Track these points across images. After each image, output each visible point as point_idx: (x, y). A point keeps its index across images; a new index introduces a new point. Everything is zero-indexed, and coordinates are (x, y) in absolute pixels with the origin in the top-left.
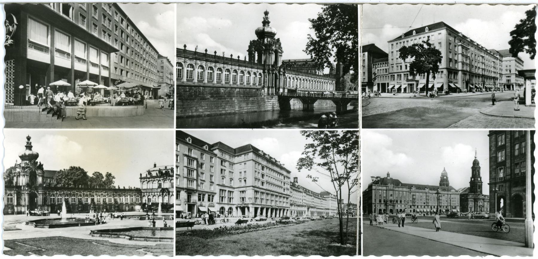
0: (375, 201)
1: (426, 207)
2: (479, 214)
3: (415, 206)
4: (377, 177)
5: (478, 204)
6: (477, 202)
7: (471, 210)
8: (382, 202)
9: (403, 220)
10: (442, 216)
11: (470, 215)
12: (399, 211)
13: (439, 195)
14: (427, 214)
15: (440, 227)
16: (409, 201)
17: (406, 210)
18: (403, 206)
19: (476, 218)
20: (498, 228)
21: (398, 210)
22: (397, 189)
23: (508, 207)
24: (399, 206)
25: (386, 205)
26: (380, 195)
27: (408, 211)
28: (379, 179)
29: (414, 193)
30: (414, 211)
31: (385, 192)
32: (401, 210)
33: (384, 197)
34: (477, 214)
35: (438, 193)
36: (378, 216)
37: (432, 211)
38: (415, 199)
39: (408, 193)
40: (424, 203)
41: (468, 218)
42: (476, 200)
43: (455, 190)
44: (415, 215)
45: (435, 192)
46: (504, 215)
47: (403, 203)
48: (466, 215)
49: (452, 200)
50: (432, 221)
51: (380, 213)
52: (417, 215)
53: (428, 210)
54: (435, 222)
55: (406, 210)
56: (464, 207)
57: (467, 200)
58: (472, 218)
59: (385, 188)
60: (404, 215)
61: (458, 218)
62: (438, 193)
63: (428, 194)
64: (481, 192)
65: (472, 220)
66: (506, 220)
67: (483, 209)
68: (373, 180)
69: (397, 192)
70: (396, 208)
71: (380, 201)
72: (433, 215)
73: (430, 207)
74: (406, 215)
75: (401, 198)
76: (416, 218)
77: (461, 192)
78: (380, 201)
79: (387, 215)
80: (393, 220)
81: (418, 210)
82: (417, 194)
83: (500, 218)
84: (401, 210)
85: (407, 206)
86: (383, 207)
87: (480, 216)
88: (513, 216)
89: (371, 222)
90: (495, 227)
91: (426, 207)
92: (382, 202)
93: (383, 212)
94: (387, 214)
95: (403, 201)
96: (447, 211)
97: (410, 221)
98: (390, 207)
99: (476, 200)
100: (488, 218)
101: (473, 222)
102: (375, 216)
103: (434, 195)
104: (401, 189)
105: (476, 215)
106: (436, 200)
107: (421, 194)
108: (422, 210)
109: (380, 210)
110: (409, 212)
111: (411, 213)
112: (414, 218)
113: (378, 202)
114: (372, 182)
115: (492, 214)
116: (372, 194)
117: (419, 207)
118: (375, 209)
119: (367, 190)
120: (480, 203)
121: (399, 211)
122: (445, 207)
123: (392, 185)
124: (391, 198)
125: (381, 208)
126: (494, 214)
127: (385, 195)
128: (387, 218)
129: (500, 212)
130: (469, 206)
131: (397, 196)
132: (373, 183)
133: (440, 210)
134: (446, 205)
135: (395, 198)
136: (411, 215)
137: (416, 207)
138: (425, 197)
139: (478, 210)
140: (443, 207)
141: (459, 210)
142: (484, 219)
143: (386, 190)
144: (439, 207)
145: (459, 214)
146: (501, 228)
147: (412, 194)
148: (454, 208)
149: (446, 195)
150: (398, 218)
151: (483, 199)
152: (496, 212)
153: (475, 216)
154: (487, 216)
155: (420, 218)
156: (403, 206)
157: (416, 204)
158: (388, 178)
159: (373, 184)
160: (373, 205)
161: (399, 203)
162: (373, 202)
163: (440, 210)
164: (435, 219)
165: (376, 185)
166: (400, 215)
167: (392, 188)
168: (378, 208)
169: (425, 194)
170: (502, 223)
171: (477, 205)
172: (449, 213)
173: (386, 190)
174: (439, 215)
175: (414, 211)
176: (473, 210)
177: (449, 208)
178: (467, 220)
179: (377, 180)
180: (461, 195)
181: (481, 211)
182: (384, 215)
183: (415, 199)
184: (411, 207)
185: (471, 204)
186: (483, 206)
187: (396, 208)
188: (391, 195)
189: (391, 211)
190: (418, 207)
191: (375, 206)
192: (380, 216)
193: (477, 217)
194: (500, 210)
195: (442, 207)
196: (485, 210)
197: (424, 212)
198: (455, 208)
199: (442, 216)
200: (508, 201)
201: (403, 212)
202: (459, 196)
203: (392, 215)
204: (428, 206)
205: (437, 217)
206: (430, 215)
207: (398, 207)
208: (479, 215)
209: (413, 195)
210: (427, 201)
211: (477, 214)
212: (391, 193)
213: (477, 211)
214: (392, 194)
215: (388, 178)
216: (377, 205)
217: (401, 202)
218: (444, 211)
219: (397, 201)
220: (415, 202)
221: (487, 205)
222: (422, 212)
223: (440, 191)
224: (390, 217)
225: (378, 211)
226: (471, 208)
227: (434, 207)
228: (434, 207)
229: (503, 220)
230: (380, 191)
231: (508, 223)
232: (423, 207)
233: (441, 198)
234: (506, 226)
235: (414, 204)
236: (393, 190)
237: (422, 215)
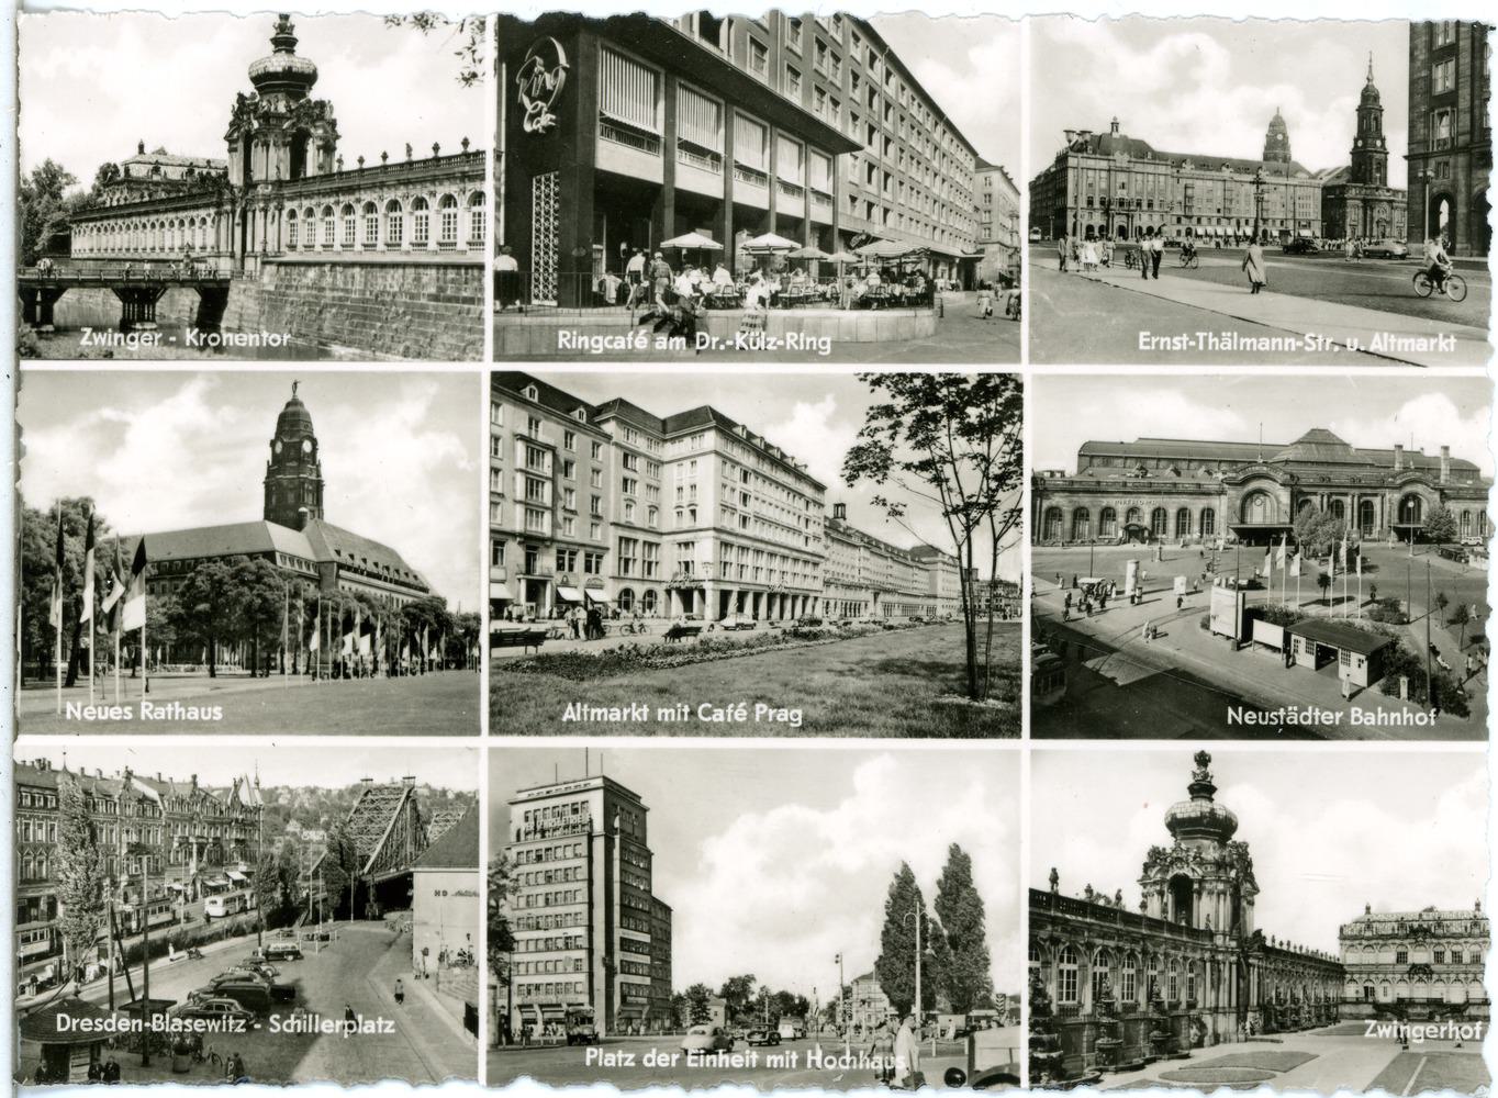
0: (1076, 202)
1: (1224, 221)
2: (1377, 243)
3: (1190, 217)
4: (1083, 133)
5: (1375, 214)
6: (1372, 209)
7: (1353, 233)
8: (1097, 205)
9: (1157, 257)
10: (1269, 248)
11: (1350, 248)
12: (1144, 231)
13: (1261, 187)
14: (1226, 242)
15: (1264, 282)
16: (1176, 205)
17: (1164, 229)
18: (1156, 217)
19: (1368, 257)
20: (1432, 287)
21: (1140, 228)
22: (1139, 167)
23: (1461, 227)
24: (1145, 217)
25: (1107, 212)
26: (1090, 185)
27: (1171, 231)
28: (1088, 137)
29: (1190, 182)
30: (1189, 232)
31: (1104, 174)
32: (1150, 230)
33: (1101, 190)
34: (1370, 243)
35: (1258, 182)
36: (1082, 246)
37: (1240, 233)
38: (1191, 198)
39: (1170, 180)
40: (1219, 211)
41: (1343, 255)
42: (1368, 204)
43: (1308, 173)
44: (1191, 245)
45: (1251, 178)
46: (1451, 252)
47: (1156, 208)
48: (1339, 246)
49: (1297, 202)
50: (1241, 263)
51: (1089, 237)
52: (1198, 244)
53: (1230, 232)
54: (1249, 265)
55: (1164, 229)
56: (1333, 227)
57: (1342, 202)
58: (1355, 255)
59: (1104, 164)
60: (1158, 244)
61: (1316, 254)
62: (1258, 182)
63: (1228, 185)
64: (1384, 180)
65: (1355, 261)
66: (1457, 265)
67: (1388, 230)
68: (1070, 141)
69: (1139, 177)
70: (1137, 223)
71: (1090, 202)
72: (1244, 246)
73: (1234, 222)
74: (1165, 245)
75: (1152, 193)
76: (1195, 253)
77: (1325, 179)
78: (1090, 202)
79: (1111, 244)
80: (1128, 257)
81: (1200, 231)
82: (1199, 183)
83: (1438, 257)
84: (1150, 230)
85: (1167, 218)
86: (1098, 220)
87: (1379, 252)
88: (1475, 252)
89: (1062, 263)
90: (1423, 284)
91: (1224, 221)
92: (1097, 205)
93: (1097, 233)
94: (1110, 240)
95: (1156, 203)
96: (1284, 233)
97: (1178, 263)
98: (1119, 221)
99: (1368, 204)
100: (1403, 257)
101: (1358, 267)
102: (1075, 246)
103: (1248, 186)
104: (1150, 169)
105: (1368, 247)
106: (1253, 201)
107: (1210, 184)
108: (1211, 230)
109: (1090, 228)
110: (1175, 234)
111: (1179, 240)
112: (1189, 253)
113: (1085, 206)
114: (1067, 144)
115: (1414, 246)
116: (1066, 181)
117: (1204, 221)
118: (1075, 224)
119: (1053, 170)
120: (1380, 213)
121: (1144, 231)
122: (1278, 223)
123: (1126, 157)
124: (1121, 194)
125: (1092, 223)
126: (1421, 245)
127: (1104, 185)
128: (1111, 252)
129: (1440, 239)
130: (1348, 220)
131: (1139, 188)
132: (1072, 148)
133: (1265, 232)
134: (1282, 216)
135: (1133, 195)
136: (1179, 244)
137: (1195, 220)
138: (1220, 193)
139: (1375, 233)
140: (1274, 221)
141: (1318, 234)
142: (1390, 258)
143: (1109, 171)
144: (1260, 223)
145: (1318, 243)
146: (1440, 286)
147: (1183, 182)
148: (1305, 226)
149: (1283, 188)
150: (1142, 252)
151: (1390, 202)
152: (1427, 241)
153: (1365, 251)
154: (1399, 250)
155: (1207, 252)
156: (1156, 217)
157: (1195, 212)
158: (1115, 135)
159: (1070, 153)
160: (1070, 214)
161: (1145, 207)
162: (1070, 203)
163: (1265, 232)
164: (1250, 258)
165: (1080, 155)
166: (1146, 245)
167: (1125, 165)
168: (1084, 221)
170: (1444, 272)
171: (1372, 218)
172: (1290, 240)
173: (1109, 171)
174: (1262, 245)
175: (1189, 232)
176: (1359, 231)
177: (1290, 225)
178: (1343, 261)
179: (1081, 140)
180: (1326, 190)
181: (1384, 236)
182: (1100, 244)
183: (1191, 198)
184: (1179, 221)
185: (1353, 215)
186: (1389, 223)
187: (1137, 223)
188: (1123, 186)
189: (1123, 232)
190: (1199, 221)
191: (1075, 216)
192: (1090, 245)
193: (1370, 254)
194: (1438, 234)
195: (1270, 222)
196: (1396, 233)
197: (1217, 236)
198: (1308, 226)
199: (1269, 248)
200: (1462, 210)
201: (1156, 235)
202: (1318, 192)
203: (1123, 242)
204: (1229, 219)
205: (1256, 250)
206: (1234, 247)
207: (1143, 220)
208: (1376, 248)
209: (1186, 187)
211: (1370, 243)
212: (1122, 178)
213: (1371, 236)
214: (1125, 181)
215: (1115, 135)
216: (1080, 213)
217: (1150, 205)
218: (1276, 233)
219: (1139, 204)
220: (1191, 207)
221: (1400, 218)
222: (1211, 237)
223: (1263, 175)
224: (1118, 248)
225: (1084, 230)
226: (1354, 227)
227: (1247, 222)
228: (1247, 222)
229: (1446, 263)
230: (1091, 173)
231: (1460, 272)
232: (1214, 221)
233: (1266, 196)
234: (1456, 282)
235: (1188, 213)
236: (1128, 171)
237: (1213, 245)
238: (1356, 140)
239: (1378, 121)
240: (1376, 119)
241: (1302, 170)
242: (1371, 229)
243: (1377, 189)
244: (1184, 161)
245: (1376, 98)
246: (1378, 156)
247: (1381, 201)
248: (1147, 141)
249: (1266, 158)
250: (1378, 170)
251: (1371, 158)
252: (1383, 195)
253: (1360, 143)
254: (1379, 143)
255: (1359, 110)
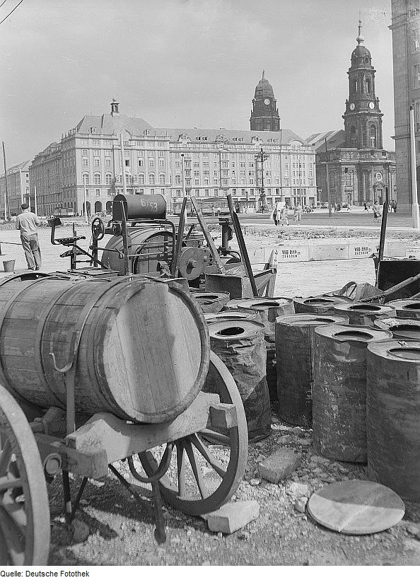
6: (368, 173)
42: (362, 170)
99: (362, 170)
116: (74, 161)
139: (372, 198)
151: (386, 165)
162: (79, 182)
226: (349, 193)
238: (348, 104)
239: (370, 82)
240: (368, 81)
242: (368, 194)
243: (372, 153)
245: (368, 59)
246: (372, 119)
247: (377, 164)
250: (373, 133)
251: (364, 122)
252: (379, 158)
253: (352, 107)
254: (372, 105)
255: (351, 72)
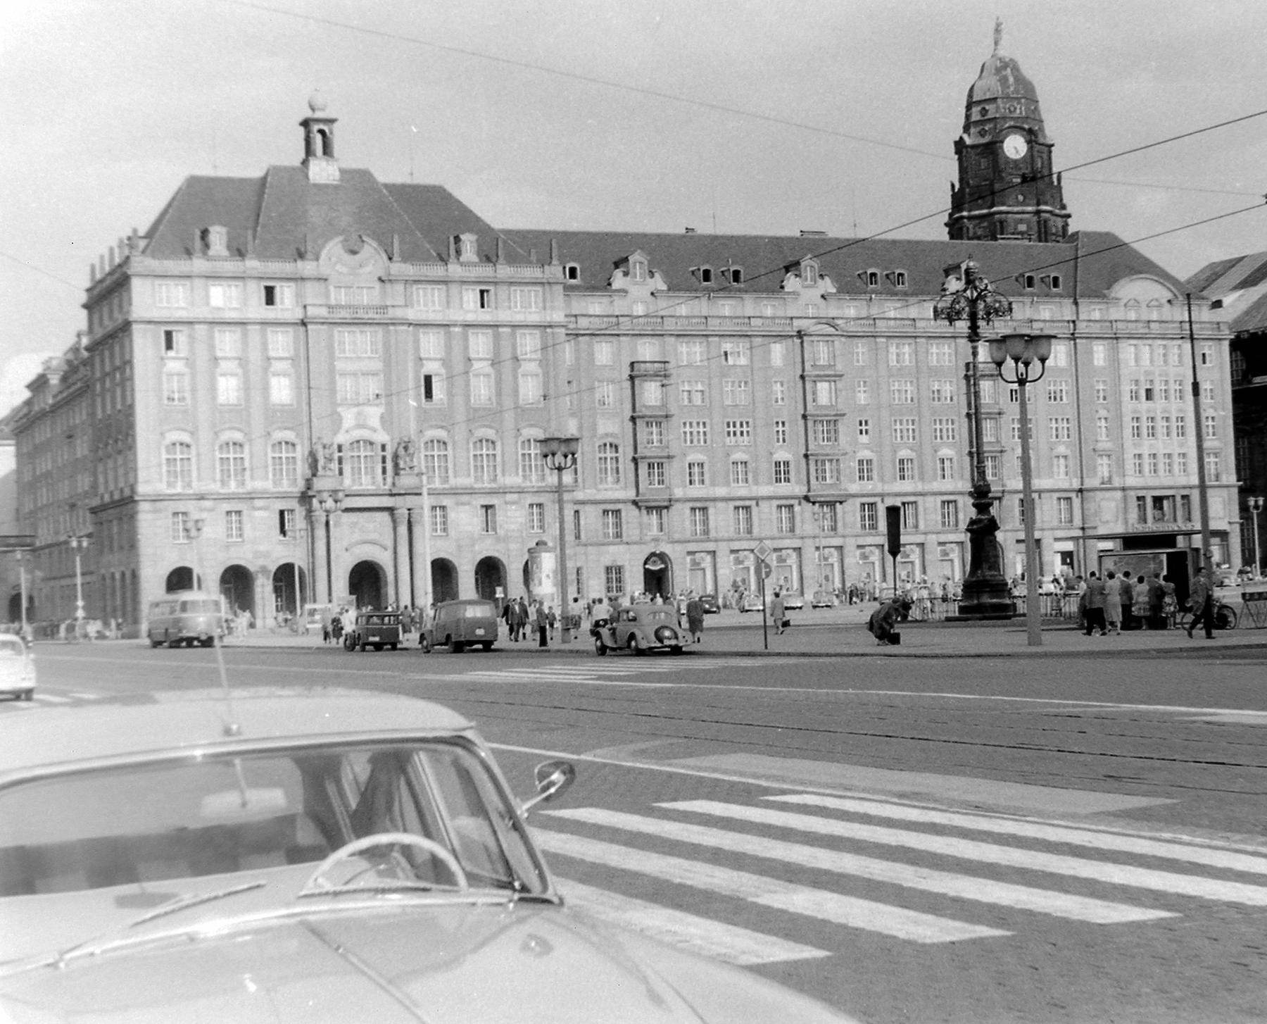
29: (647, 351)
43: (1162, 276)
63: (820, 353)
82: (690, 353)
137: (680, 518)
158: (322, 171)
167: (369, 296)
169: (778, 351)
210: (818, 445)
220: (657, 465)
235: (651, 490)
241: (1138, 266)
244: (621, 262)
248: (449, 188)
249: (956, 228)
